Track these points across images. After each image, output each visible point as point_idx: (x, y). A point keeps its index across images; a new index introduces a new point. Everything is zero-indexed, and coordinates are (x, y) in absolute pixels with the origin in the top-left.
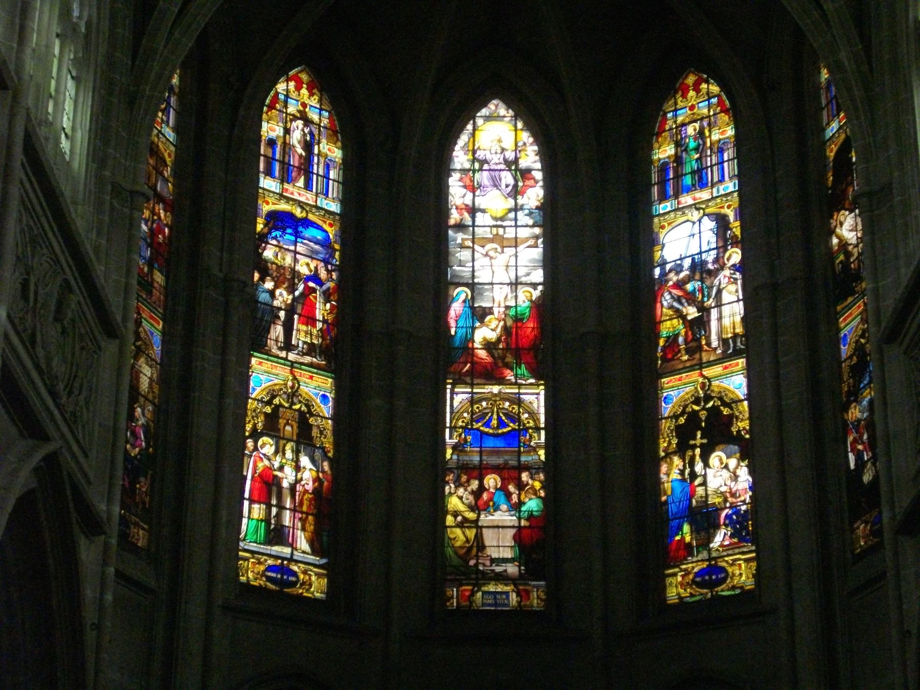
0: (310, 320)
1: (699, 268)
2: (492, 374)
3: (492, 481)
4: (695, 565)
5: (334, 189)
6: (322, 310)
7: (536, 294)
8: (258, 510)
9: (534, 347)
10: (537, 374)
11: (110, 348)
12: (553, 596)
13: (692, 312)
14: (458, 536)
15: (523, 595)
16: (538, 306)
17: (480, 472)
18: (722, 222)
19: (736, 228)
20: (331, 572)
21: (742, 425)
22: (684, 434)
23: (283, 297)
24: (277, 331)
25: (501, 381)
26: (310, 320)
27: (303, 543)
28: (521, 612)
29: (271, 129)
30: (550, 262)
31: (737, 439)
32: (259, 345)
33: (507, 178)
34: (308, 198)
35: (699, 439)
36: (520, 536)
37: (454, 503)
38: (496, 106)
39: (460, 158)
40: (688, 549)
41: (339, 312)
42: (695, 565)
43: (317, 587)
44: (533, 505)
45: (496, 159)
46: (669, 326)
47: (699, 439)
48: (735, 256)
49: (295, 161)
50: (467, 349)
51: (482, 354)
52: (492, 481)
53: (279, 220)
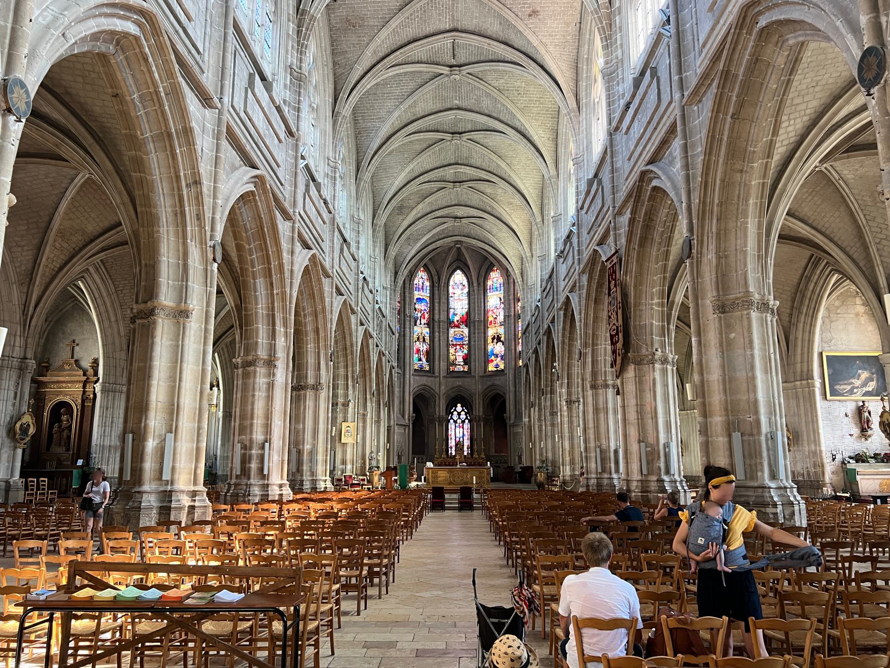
0: (424, 318)
1: (496, 307)
2: (458, 327)
3: (458, 347)
4: (495, 363)
5: (428, 291)
6: (427, 316)
7: (466, 310)
8: (417, 355)
9: (466, 321)
10: (466, 326)
11: (394, 336)
12: (469, 368)
13: (495, 316)
14: (452, 358)
15: (464, 368)
16: (467, 313)
17: (456, 345)
18: (501, 300)
19: (502, 301)
20: (429, 365)
21: (502, 339)
22: (493, 339)
23: (419, 315)
24: (418, 321)
25: (460, 328)
26: (424, 318)
27: (424, 360)
28: (463, 371)
29: (416, 282)
30: (469, 304)
31: (502, 341)
32: (415, 325)
33: (461, 287)
34: (423, 294)
35: (495, 341)
36: (463, 358)
37: (451, 351)
38: (458, 272)
39: (451, 283)
40: (492, 361)
41: (430, 315)
42: (495, 363)
43: (427, 368)
44: (466, 351)
45: (458, 283)
46: (490, 319)
47: (495, 341)
48: (502, 306)
49: (420, 287)
50: (453, 322)
51: (456, 322)
52: (458, 347)
53: (419, 300)
